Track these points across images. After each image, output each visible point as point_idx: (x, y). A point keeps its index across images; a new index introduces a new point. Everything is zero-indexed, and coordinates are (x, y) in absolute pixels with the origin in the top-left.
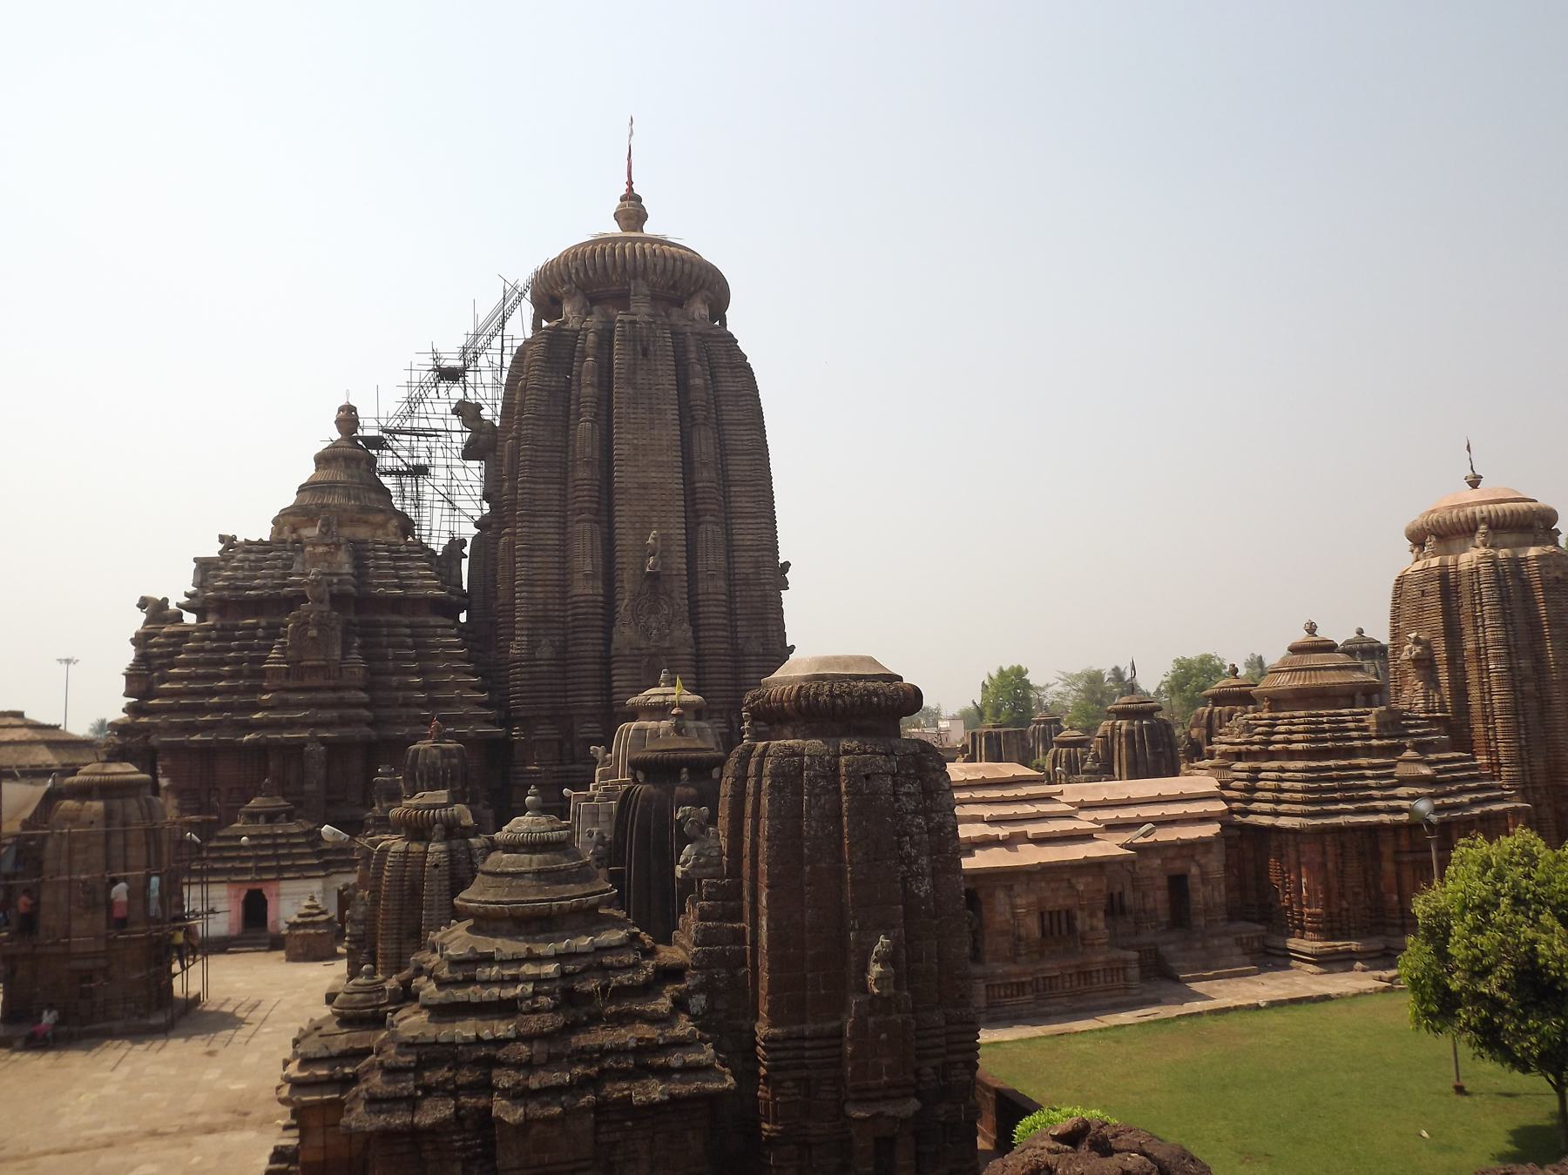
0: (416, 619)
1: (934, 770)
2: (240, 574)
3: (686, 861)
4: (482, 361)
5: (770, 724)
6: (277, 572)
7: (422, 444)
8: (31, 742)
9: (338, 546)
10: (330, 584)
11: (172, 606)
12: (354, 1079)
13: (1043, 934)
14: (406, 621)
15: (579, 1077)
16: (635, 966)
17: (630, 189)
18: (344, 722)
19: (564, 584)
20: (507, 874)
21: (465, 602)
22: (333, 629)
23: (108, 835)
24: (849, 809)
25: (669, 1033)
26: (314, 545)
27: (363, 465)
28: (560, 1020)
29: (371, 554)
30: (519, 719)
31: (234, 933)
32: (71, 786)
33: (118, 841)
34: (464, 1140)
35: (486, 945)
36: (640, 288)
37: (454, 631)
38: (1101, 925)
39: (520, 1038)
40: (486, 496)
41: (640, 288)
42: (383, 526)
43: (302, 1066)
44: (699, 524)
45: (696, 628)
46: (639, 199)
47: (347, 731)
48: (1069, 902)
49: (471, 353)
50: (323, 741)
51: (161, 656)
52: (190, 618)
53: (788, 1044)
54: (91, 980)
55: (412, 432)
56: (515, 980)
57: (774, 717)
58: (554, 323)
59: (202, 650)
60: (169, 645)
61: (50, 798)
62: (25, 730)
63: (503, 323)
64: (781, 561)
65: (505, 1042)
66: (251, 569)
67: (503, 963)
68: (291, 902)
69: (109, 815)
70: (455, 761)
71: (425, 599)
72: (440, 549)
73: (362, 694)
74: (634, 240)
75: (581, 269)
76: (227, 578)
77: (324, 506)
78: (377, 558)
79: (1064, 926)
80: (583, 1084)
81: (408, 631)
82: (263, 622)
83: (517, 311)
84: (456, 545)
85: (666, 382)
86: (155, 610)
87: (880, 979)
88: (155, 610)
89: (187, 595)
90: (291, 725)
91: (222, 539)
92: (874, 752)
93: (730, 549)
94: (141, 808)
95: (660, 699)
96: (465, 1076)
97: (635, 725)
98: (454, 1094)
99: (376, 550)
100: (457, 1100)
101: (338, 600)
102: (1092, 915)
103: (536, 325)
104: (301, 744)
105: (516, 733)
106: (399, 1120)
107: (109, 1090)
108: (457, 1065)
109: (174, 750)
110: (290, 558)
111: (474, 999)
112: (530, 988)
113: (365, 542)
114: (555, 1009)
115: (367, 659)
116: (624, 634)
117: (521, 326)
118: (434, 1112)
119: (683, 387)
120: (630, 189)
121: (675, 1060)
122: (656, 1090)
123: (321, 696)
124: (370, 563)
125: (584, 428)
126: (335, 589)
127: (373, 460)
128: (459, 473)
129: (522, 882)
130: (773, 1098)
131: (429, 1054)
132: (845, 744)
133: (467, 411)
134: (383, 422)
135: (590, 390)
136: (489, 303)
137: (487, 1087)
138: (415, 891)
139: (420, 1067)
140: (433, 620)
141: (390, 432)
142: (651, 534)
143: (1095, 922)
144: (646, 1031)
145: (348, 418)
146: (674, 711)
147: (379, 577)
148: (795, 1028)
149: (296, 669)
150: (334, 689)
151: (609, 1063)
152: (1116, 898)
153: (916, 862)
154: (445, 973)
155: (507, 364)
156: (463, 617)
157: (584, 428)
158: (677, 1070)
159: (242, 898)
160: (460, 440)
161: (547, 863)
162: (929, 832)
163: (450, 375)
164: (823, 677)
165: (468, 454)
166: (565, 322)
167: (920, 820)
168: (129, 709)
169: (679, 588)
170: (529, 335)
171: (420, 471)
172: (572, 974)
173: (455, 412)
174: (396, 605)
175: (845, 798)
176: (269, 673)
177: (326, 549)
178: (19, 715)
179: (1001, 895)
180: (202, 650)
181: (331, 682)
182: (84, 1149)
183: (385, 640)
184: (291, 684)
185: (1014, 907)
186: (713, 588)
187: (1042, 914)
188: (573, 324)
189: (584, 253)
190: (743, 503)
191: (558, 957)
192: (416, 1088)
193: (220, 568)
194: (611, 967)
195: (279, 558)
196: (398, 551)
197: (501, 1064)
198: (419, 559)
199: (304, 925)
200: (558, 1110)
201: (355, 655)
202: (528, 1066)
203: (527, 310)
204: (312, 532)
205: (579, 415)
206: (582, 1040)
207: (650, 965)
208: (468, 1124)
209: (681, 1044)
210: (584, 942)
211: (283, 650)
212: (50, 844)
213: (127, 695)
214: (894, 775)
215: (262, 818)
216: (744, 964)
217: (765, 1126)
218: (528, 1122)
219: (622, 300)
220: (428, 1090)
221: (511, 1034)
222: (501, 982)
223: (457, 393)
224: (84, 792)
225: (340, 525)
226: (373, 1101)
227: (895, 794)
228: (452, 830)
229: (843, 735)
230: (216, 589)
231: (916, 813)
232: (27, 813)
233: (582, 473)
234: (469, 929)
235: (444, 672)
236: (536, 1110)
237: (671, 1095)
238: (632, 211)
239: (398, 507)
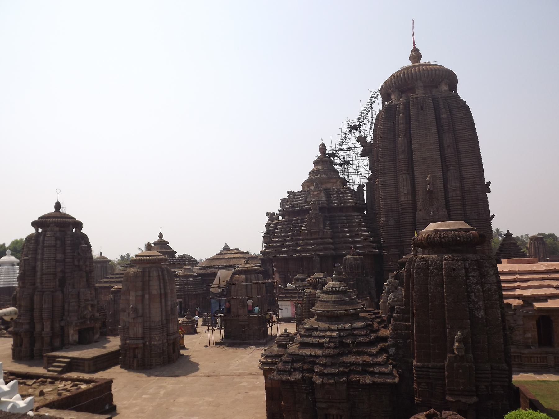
0: (347, 214)
1: (486, 267)
2: (292, 203)
3: (390, 299)
4: (366, 121)
7: (347, 154)
8: (240, 258)
9: (321, 191)
10: (319, 204)
11: (275, 215)
12: (276, 363)
14: (344, 214)
15: (341, 371)
16: (366, 335)
17: (414, 47)
18: (325, 249)
20: (325, 301)
21: (365, 207)
24: (446, 282)
25: (375, 360)
26: (313, 192)
27: (328, 163)
28: (336, 352)
29: (332, 193)
32: (237, 270)
33: (249, 287)
34: (306, 387)
35: (317, 324)
39: (323, 356)
40: (370, 169)
42: (336, 183)
43: (264, 358)
45: (449, 211)
47: (326, 252)
49: (361, 119)
50: (319, 256)
51: (273, 230)
52: (281, 218)
53: (423, 369)
54: (244, 327)
55: (344, 150)
56: (324, 337)
59: (283, 228)
61: (234, 274)
63: (372, 106)
64: (486, 181)
65: (319, 357)
66: (296, 201)
67: (321, 331)
69: (247, 279)
70: (359, 262)
71: (350, 207)
72: (355, 189)
73: (330, 240)
74: (415, 67)
75: (397, 82)
76: (289, 205)
77: (316, 178)
78: (334, 194)
80: (343, 374)
81: (345, 218)
82: (300, 218)
83: (377, 101)
84: (361, 187)
86: (270, 215)
87: (458, 348)
88: (270, 215)
90: (309, 251)
91: (288, 192)
92: (457, 260)
93: (462, 179)
94: (255, 277)
96: (306, 366)
98: (302, 371)
99: (333, 191)
100: (303, 374)
101: (322, 209)
104: (312, 257)
106: (285, 378)
107: (244, 360)
108: (305, 363)
109: (277, 259)
110: (307, 197)
111: (311, 342)
112: (328, 340)
113: (330, 189)
114: (336, 348)
116: (420, 214)
117: (378, 107)
118: (296, 376)
119: (438, 118)
120: (414, 47)
121: (376, 370)
122: (368, 379)
124: (332, 196)
125: (401, 140)
126: (320, 205)
127: (332, 161)
128: (360, 162)
129: (329, 304)
130: (419, 388)
131: (296, 358)
132: (445, 256)
134: (334, 148)
135: (402, 126)
136: (366, 101)
137: (311, 371)
139: (293, 362)
140: (353, 214)
141: (336, 151)
142: (428, 177)
144: (367, 358)
145: (323, 148)
147: (335, 200)
148: (426, 364)
150: (322, 238)
151: (353, 368)
154: (303, 333)
155: (374, 119)
156: (365, 212)
157: (401, 140)
158: (377, 373)
160: (360, 150)
161: (337, 298)
162: (483, 291)
163: (355, 128)
164: (438, 231)
165: (362, 155)
166: (392, 102)
167: (479, 287)
168: (265, 247)
170: (381, 109)
171: (347, 163)
172: (343, 336)
173: (357, 140)
174: (341, 209)
178: (238, 250)
180: (283, 228)
181: (320, 236)
182: (233, 376)
183: (337, 222)
184: (308, 237)
188: (395, 102)
189: (397, 75)
191: (338, 330)
192: (291, 368)
193: (288, 202)
194: (357, 335)
195: (304, 197)
197: (317, 364)
198: (348, 193)
200: (333, 381)
202: (325, 365)
203: (380, 100)
205: (399, 135)
206: (346, 359)
207: (373, 335)
208: (307, 382)
209: (379, 364)
210: (348, 326)
211: (305, 227)
212: (232, 288)
215: (300, 281)
216: (409, 338)
217: (416, 398)
218: (323, 384)
219: (412, 90)
220: (295, 370)
221: (321, 355)
222: (320, 337)
223: (357, 134)
224: (240, 272)
225: (322, 184)
226: (279, 371)
227: (467, 277)
229: (444, 253)
230: (286, 208)
231: (477, 284)
232: (228, 279)
234: (316, 320)
235: (358, 231)
236: (326, 380)
237: (374, 382)
238: (416, 55)
239: (341, 176)
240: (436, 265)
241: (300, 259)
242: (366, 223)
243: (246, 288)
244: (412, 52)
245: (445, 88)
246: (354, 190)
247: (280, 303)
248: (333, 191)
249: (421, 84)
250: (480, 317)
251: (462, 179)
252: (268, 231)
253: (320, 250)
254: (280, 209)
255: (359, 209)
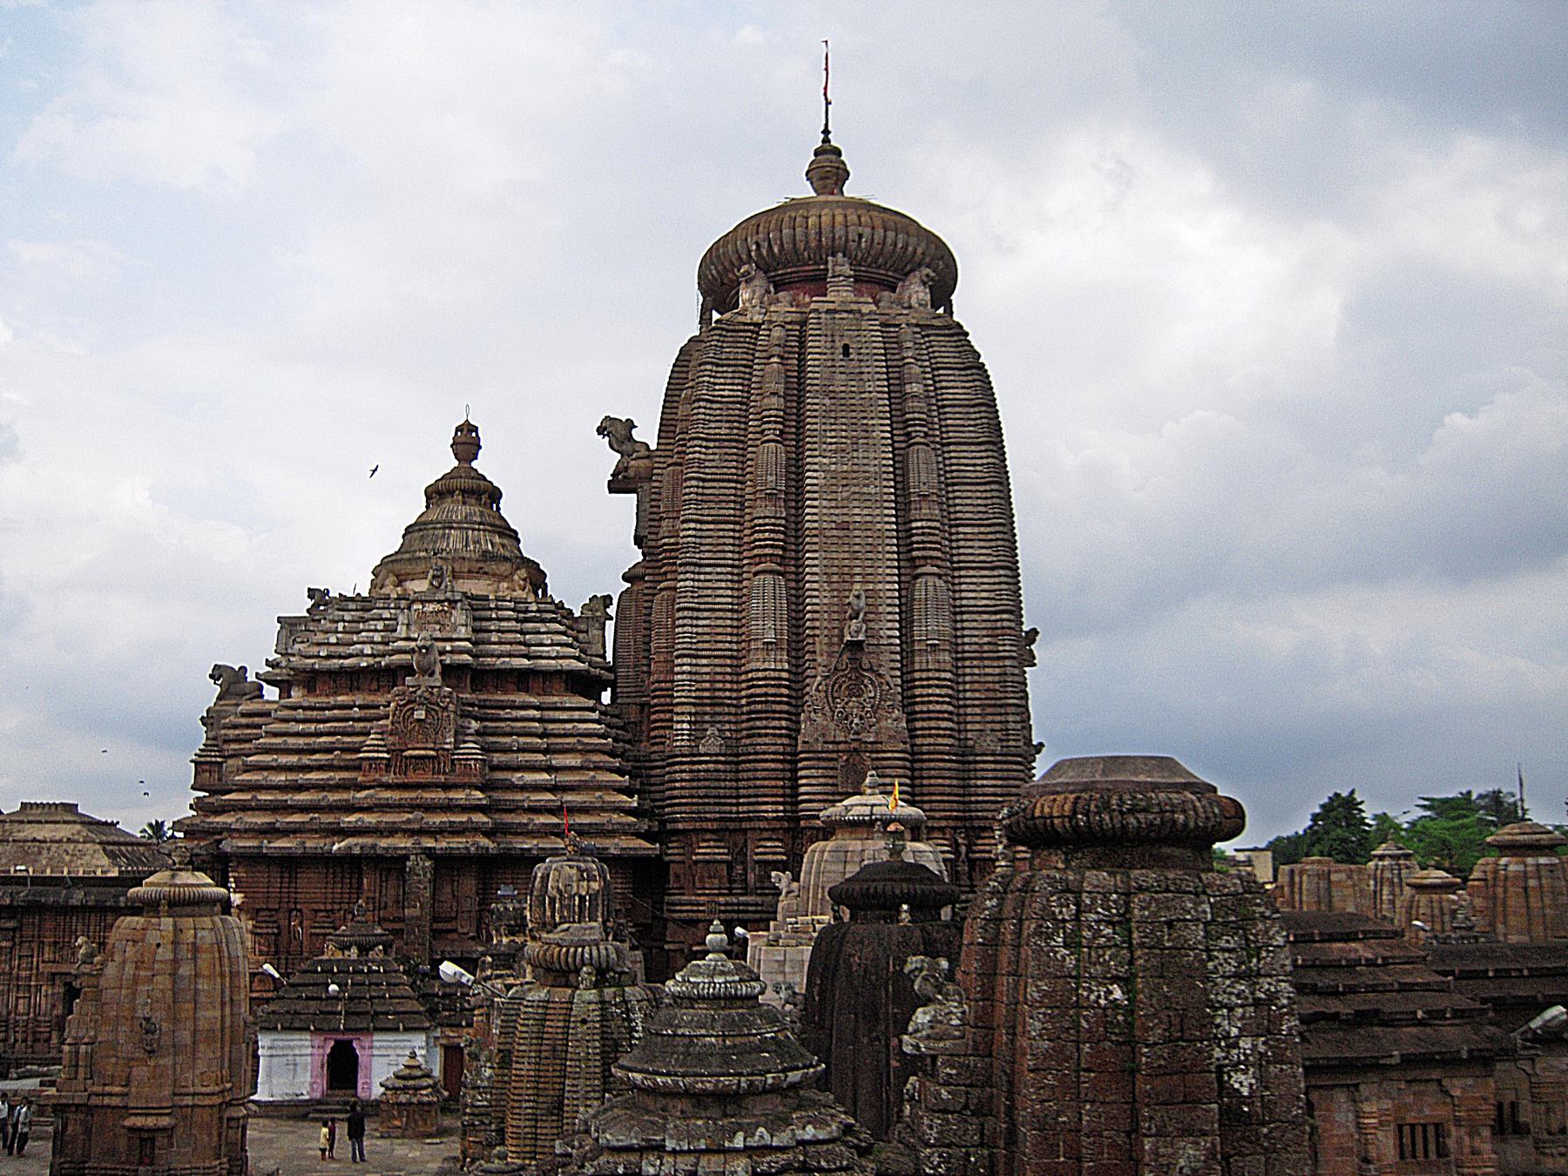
1: (1264, 917)
2: (333, 640)
3: (916, 1031)
5: (1033, 847)
6: (377, 637)
9: (452, 603)
11: (251, 677)
13: (1402, 1157)
17: (826, 141)
19: (737, 659)
22: (445, 709)
23: (176, 962)
30: (676, 832)
31: (318, 1095)
33: (185, 970)
36: (840, 266)
37: (596, 715)
38: (1487, 1147)
40: (638, 541)
41: (840, 266)
44: (916, 577)
46: (838, 153)
48: (1442, 1113)
50: (429, 853)
52: (272, 693)
57: (1035, 836)
58: (727, 316)
60: (247, 726)
62: (78, 827)
68: (385, 1061)
70: (595, 886)
71: (559, 673)
73: (479, 795)
79: (1432, 1147)
81: (537, 714)
85: (876, 387)
86: (230, 680)
88: (230, 680)
89: (268, 663)
91: (312, 593)
95: (867, 810)
97: (830, 845)
101: (451, 673)
102: (1470, 1135)
103: (704, 319)
105: (674, 852)
113: (486, 598)
115: (485, 750)
116: (816, 726)
120: (826, 141)
123: (425, 795)
126: (448, 659)
133: (616, 432)
138: (559, 1053)
143: (1477, 1142)
146: (892, 828)
149: (397, 760)
150: (446, 787)
152: (1507, 1109)
153: (1236, 1045)
156: (606, 697)
159: (328, 1051)
168: (198, 805)
169: (888, 664)
174: (523, 679)
175: (1139, 953)
176: (365, 764)
177: (438, 607)
179: (1341, 1096)
181: (442, 778)
184: (389, 778)
185: (1358, 1115)
186: (933, 664)
187: (1400, 1127)
190: (974, 548)
191: (747, 1150)
196: (527, 611)
199: (406, 1088)
201: (471, 746)
204: (419, 586)
213: (193, 788)
214: (1206, 924)
219: (818, 283)
225: (455, 576)
227: (1207, 950)
228: (603, 975)
231: (1238, 976)
233: (764, 510)
238: (828, 168)
240: (1108, 909)
241: (351, 864)
242: (616, 740)
243: (174, 974)
244: (816, 154)
245: (921, 295)
246: (570, 612)
247: (264, 1040)
248: (498, 609)
249: (847, 270)
250: (1245, 1092)
251: (957, 611)
252: (213, 743)
253: (434, 832)
254: (273, 656)
255: (585, 684)
